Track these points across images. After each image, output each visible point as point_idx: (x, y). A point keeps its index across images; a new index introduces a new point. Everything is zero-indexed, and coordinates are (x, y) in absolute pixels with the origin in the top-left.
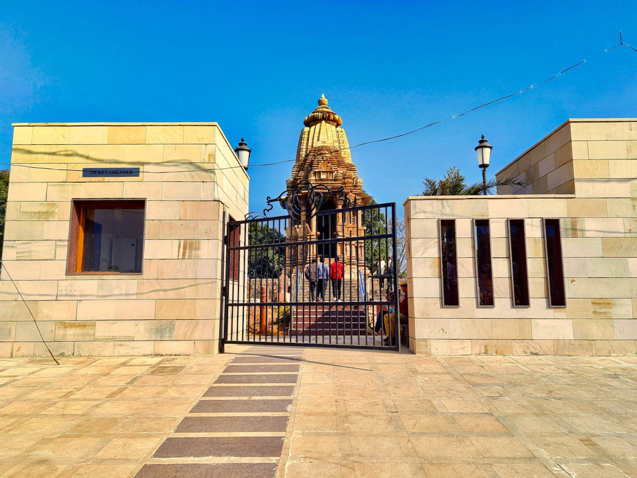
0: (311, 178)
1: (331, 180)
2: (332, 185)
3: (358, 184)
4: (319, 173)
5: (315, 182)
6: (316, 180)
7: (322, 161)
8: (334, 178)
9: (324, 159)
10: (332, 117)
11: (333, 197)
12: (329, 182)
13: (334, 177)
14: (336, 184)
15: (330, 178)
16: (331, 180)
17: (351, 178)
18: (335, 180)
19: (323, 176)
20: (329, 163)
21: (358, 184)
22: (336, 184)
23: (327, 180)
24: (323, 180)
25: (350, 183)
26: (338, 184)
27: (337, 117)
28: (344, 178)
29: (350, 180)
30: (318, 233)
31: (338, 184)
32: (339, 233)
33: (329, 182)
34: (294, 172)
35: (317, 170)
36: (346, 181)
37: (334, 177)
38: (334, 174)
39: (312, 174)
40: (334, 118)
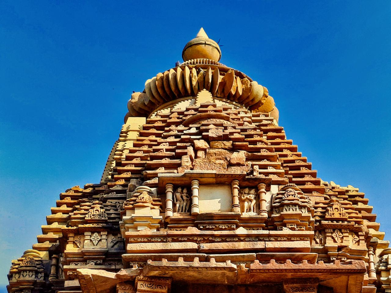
0: (139, 213)
1: (247, 223)
4: (184, 186)
5: (163, 232)
6: (164, 224)
7: (201, 144)
8: (265, 215)
9: (211, 134)
10: (238, 86)
12: (241, 231)
13: (265, 206)
15: (253, 214)
16: (247, 223)
17: (355, 231)
18: (270, 224)
22: (277, 238)
23: (230, 220)
26: (290, 238)
27: (259, 89)
28: (321, 230)
29: (350, 242)
31: (290, 238)
33: (241, 231)
34: (55, 225)
36: (329, 243)
37: (265, 206)
38: (266, 197)
39: (146, 196)
40: (248, 90)
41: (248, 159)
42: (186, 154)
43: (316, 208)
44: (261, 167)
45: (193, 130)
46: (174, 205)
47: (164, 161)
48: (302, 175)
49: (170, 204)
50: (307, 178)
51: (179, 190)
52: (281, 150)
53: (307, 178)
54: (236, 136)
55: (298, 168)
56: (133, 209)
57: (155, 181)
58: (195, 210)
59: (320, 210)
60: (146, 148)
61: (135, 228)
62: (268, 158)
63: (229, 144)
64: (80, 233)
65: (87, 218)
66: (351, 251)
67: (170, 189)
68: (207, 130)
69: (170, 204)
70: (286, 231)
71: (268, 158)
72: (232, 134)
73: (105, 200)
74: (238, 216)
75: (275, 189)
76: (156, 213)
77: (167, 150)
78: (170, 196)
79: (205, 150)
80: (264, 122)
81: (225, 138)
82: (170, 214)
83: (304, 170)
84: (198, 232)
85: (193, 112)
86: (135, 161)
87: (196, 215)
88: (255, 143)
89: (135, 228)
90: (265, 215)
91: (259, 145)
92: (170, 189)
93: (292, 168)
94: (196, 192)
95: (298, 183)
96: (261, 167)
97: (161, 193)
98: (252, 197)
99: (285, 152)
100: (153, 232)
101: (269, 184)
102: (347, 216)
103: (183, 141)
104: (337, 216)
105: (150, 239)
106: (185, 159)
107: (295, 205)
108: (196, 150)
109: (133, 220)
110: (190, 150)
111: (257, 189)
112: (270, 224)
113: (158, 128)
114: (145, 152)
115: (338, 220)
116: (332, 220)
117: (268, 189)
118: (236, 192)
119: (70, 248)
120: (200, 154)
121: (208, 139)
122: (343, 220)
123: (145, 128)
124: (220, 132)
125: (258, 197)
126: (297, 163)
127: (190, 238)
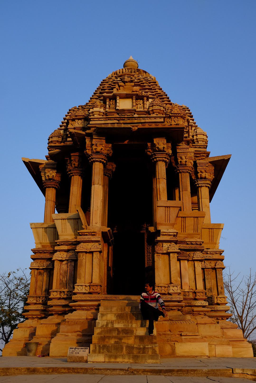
0: (95, 109)
1: (139, 113)
2: (143, 121)
3: (199, 136)
6: (106, 114)
7: (122, 84)
9: (125, 80)
15: (142, 110)
19: (124, 104)
20: (135, 85)
21: (199, 136)
24: (123, 111)
26: (155, 118)
30: (106, 229)
31: (155, 118)
32: (160, 228)
33: (136, 116)
41: (140, 90)
42: (115, 88)
46: (109, 106)
47: (106, 91)
48: (163, 98)
49: (108, 106)
51: (112, 101)
52: (155, 89)
53: (165, 99)
54: (136, 81)
55: (162, 96)
56: (93, 108)
57: (102, 98)
58: (117, 108)
59: (169, 110)
61: (94, 115)
62: (148, 89)
63: (133, 84)
64: (73, 120)
65: (76, 114)
67: (108, 100)
69: (108, 106)
71: (148, 89)
74: (135, 110)
75: (150, 100)
76: (102, 110)
77: (108, 87)
78: (108, 103)
79: (123, 86)
80: (149, 80)
81: (131, 81)
82: (107, 110)
83: (164, 97)
84: (118, 116)
86: (97, 95)
87: (118, 110)
88: (143, 83)
89: (94, 115)
90: (146, 110)
91: (145, 84)
92: (108, 100)
93: (159, 96)
94: (118, 101)
95: (160, 99)
96: (145, 92)
97: (105, 103)
98: (141, 103)
99: (157, 90)
101: (148, 98)
102: (180, 112)
103: (115, 83)
104: (176, 112)
107: (158, 105)
108: (119, 86)
109: (92, 112)
110: (117, 86)
111: (143, 100)
112: (148, 113)
115: (176, 114)
116: (174, 114)
118: (134, 100)
120: (121, 88)
121: (124, 82)
122: (178, 114)
123: (102, 83)
124: (129, 79)
126: (161, 94)
127: (115, 119)
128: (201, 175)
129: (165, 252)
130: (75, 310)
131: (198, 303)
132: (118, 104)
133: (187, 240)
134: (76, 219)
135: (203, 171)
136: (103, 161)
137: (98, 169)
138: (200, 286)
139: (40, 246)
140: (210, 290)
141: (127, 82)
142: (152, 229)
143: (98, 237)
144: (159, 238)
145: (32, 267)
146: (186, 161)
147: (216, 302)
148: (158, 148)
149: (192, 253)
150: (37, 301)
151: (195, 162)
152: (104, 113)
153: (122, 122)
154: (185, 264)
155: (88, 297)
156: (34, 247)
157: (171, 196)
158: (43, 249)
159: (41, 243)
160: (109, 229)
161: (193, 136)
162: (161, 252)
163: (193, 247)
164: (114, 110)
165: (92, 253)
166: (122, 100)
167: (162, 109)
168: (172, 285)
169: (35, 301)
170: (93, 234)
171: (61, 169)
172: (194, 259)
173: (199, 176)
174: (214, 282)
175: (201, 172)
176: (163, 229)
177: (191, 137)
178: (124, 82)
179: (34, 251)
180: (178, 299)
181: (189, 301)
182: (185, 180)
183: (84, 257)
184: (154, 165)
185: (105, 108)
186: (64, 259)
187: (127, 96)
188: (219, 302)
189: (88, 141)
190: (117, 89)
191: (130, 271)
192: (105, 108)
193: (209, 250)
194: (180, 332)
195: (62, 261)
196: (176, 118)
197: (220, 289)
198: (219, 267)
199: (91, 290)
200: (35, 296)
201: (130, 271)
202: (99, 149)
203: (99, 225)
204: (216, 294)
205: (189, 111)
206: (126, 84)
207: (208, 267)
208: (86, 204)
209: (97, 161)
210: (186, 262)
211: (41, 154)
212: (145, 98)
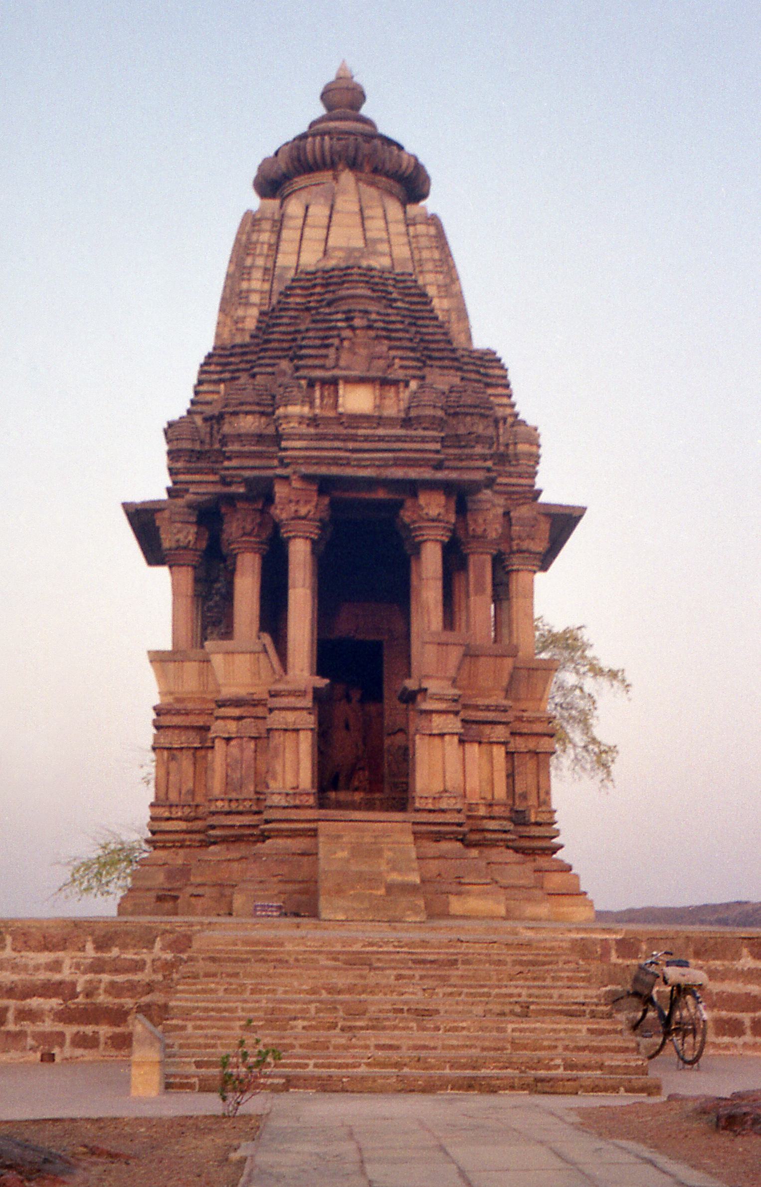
6: (314, 421)
7: (347, 333)
9: (357, 322)
11: (400, 505)
12: (381, 432)
14: (412, 439)
17: (483, 416)
19: (357, 400)
20: (377, 337)
22: (412, 439)
25: (479, 439)
26: (423, 440)
31: (423, 440)
33: (381, 432)
35: (318, 373)
43: (451, 392)
44: (402, 358)
45: (339, 316)
49: (318, 402)
50: (445, 354)
54: (381, 325)
60: (292, 313)
63: (372, 333)
64: (235, 414)
66: (479, 436)
68: (352, 319)
69: (318, 402)
70: (420, 432)
72: (375, 321)
73: (254, 376)
74: (380, 418)
75: (413, 385)
78: (317, 394)
81: (370, 327)
82: (317, 411)
85: (336, 273)
94: (341, 392)
96: (402, 358)
100: (304, 429)
105: (301, 437)
106: (332, 352)
110: (336, 342)
113: (302, 288)
114: (291, 317)
117: (407, 385)
119: (226, 429)
120: (346, 344)
121: (353, 328)
125: (397, 393)
126: (437, 337)
127: (336, 438)
128: (518, 545)
129: (435, 732)
130: (269, 838)
131: (492, 825)
132: (341, 400)
133: (480, 702)
134: (254, 653)
135: (524, 535)
136: (313, 536)
137: (300, 553)
138: (501, 791)
139: (170, 699)
140: (524, 796)
141: (358, 328)
142: (411, 684)
143: (308, 702)
144: (426, 706)
145: (156, 746)
146: (485, 530)
147: (533, 820)
148: (427, 514)
149: (487, 729)
150: (171, 812)
151: (506, 514)
152: (309, 419)
153: (350, 445)
154: (473, 750)
155: (293, 814)
156: (156, 700)
157: (449, 621)
158: (178, 706)
159: (171, 693)
160: (327, 681)
161: (507, 445)
162: (428, 732)
163: (491, 716)
164: (332, 414)
165: (297, 731)
166: (349, 388)
167: (440, 413)
168: (447, 794)
169: (167, 814)
170: (301, 694)
171: (204, 525)
172: (491, 740)
173: (515, 548)
174: (531, 780)
175: (520, 538)
176: (433, 686)
177: (502, 448)
178: (353, 328)
179: (158, 711)
180: (457, 821)
181: (479, 822)
182: (480, 567)
183: (282, 738)
184: (417, 549)
185: (312, 405)
186: (233, 736)
187: (361, 381)
188: (539, 819)
189: (280, 491)
190: (337, 349)
191: (362, 761)
192: (312, 405)
193: (525, 714)
194: (457, 878)
195: (228, 740)
196: (468, 419)
197: (542, 796)
198: (543, 750)
199: (297, 802)
200: (168, 803)
201: (362, 761)
202: (303, 511)
203: (306, 674)
204: (536, 804)
205: (502, 367)
206: (358, 332)
207: (522, 750)
208: (273, 617)
209: (300, 537)
210: (476, 746)
211: (153, 483)
212: (402, 385)
